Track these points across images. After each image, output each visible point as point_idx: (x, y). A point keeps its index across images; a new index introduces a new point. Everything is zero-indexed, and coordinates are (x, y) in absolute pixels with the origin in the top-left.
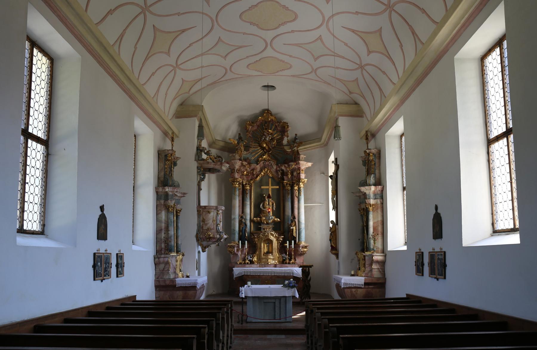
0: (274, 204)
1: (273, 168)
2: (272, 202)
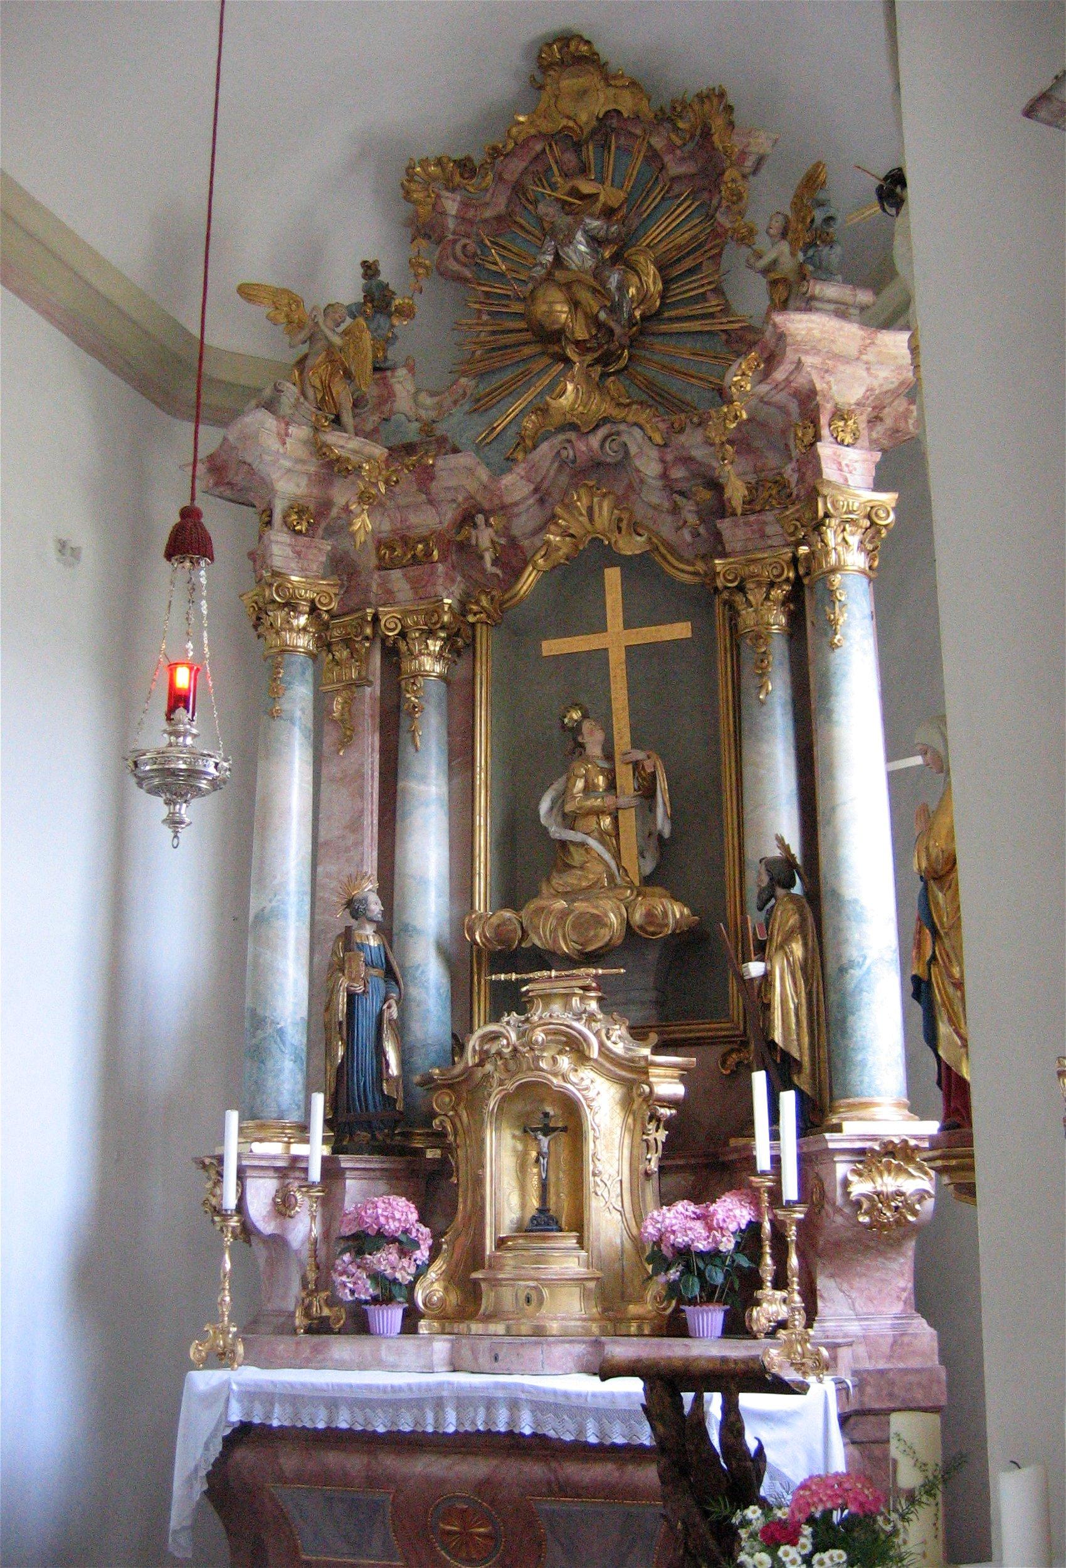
0: (662, 784)
1: (642, 481)
2: (636, 765)
